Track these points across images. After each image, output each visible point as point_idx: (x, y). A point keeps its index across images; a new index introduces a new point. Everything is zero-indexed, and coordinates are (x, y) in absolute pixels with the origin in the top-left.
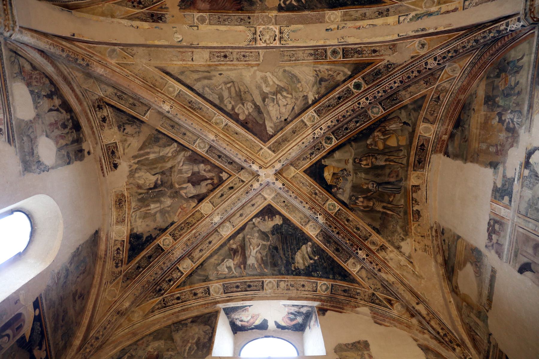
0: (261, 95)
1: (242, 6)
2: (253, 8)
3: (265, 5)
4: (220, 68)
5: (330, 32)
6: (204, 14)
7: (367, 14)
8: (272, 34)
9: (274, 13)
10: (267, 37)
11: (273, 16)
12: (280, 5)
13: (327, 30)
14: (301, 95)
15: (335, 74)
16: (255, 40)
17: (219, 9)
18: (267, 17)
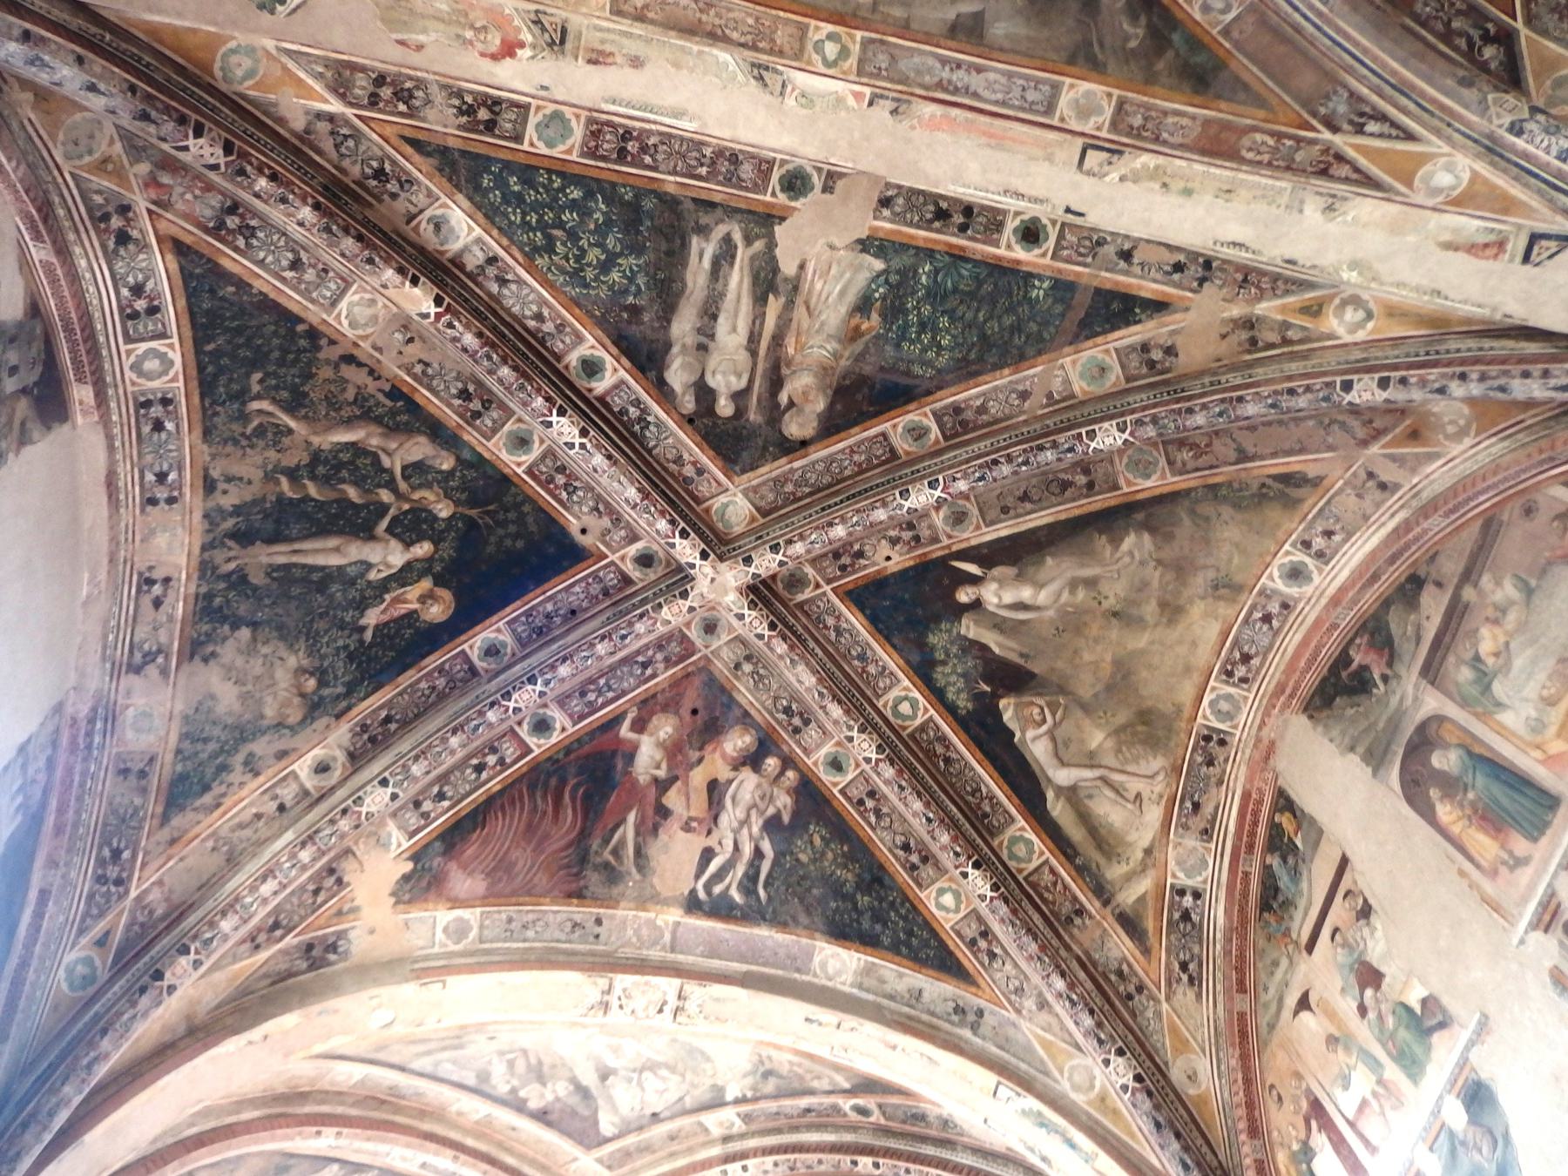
0: (597, 1070)
1: (582, 883)
2: (615, 891)
3: (652, 886)
4: (491, 1028)
5: (815, 1025)
6: (465, 914)
7: (926, 995)
8: (657, 997)
9: (673, 915)
10: (638, 1002)
11: (667, 924)
12: (693, 892)
13: (807, 1020)
14: (709, 1082)
15: (808, 1077)
16: (606, 1007)
17: (513, 894)
18: (651, 924)
